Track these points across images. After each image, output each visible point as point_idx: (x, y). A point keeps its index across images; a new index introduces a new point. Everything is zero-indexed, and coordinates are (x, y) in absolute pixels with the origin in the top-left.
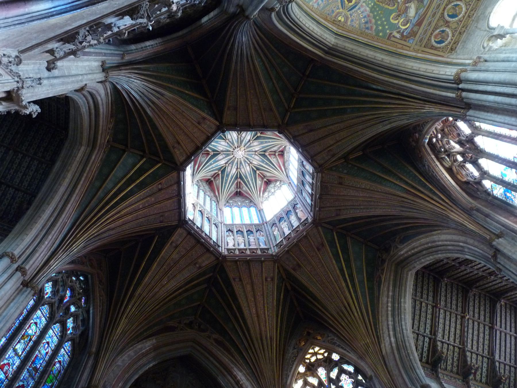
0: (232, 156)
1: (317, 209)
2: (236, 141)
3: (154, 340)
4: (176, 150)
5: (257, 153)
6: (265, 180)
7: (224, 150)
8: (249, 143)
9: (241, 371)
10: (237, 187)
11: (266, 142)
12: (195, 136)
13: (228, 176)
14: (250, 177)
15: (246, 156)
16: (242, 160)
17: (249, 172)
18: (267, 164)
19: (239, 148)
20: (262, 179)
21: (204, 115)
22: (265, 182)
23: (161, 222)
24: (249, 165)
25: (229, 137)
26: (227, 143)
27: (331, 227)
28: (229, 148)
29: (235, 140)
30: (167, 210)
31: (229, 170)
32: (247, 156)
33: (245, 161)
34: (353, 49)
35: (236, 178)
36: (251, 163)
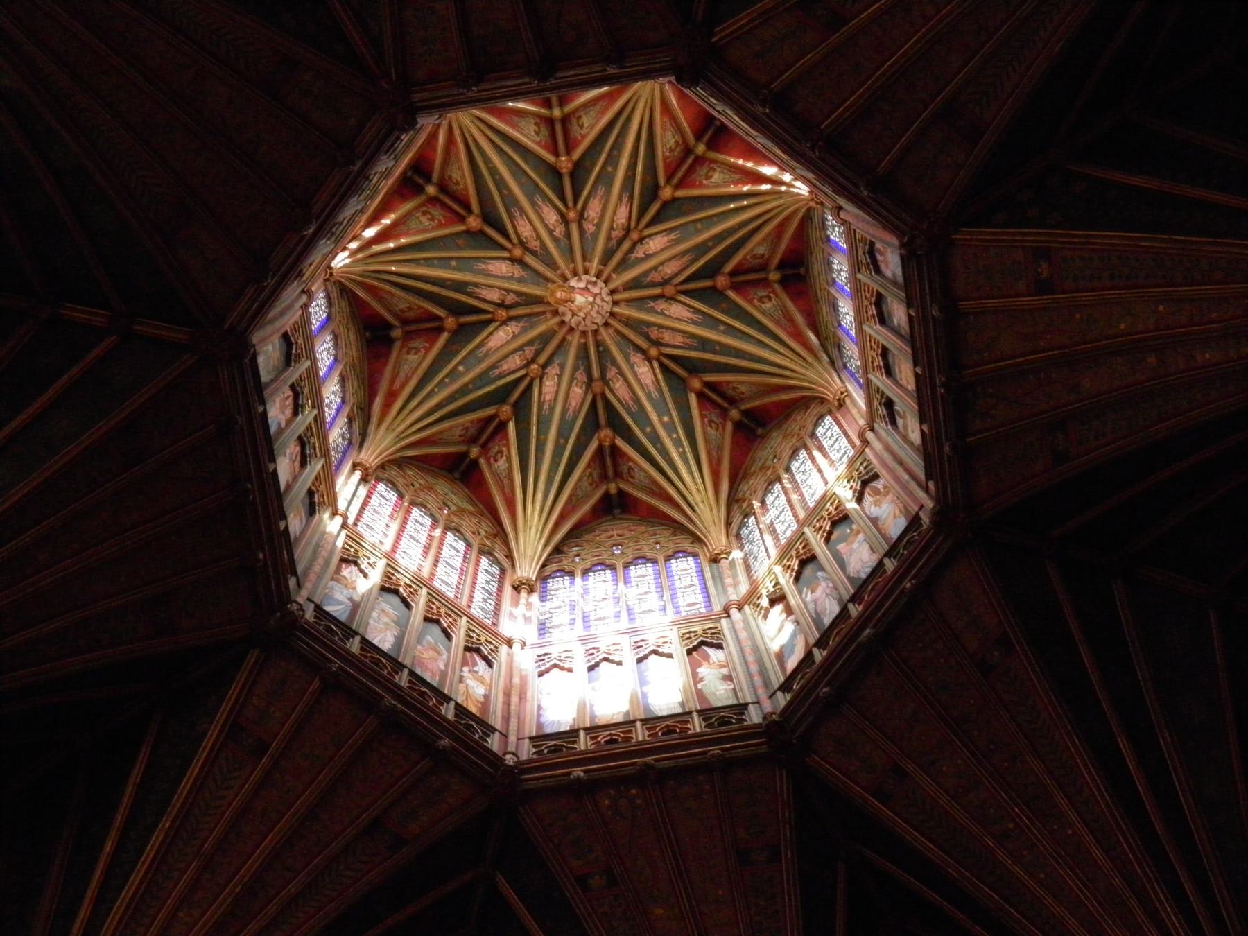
0: (605, 335)
1: (611, 70)
2: (532, 327)
5: (572, 215)
6: (701, 149)
7: (581, 376)
8: (529, 259)
10: (764, 283)
11: (500, 183)
13: (704, 344)
14: (698, 232)
15: (595, 265)
16: (618, 281)
17: (672, 236)
18: (613, 160)
19: (561, 309)
20: (700, 160)
22: (711, 146)
24: (641, 240)
25: (516, 361)
26: (544, 366)
28: (566, 354)
29: (524, 330)
31: (679, 339)
32: (596, 261)
33: (624, 265)
35: (712, 296)
36: (628, 230)
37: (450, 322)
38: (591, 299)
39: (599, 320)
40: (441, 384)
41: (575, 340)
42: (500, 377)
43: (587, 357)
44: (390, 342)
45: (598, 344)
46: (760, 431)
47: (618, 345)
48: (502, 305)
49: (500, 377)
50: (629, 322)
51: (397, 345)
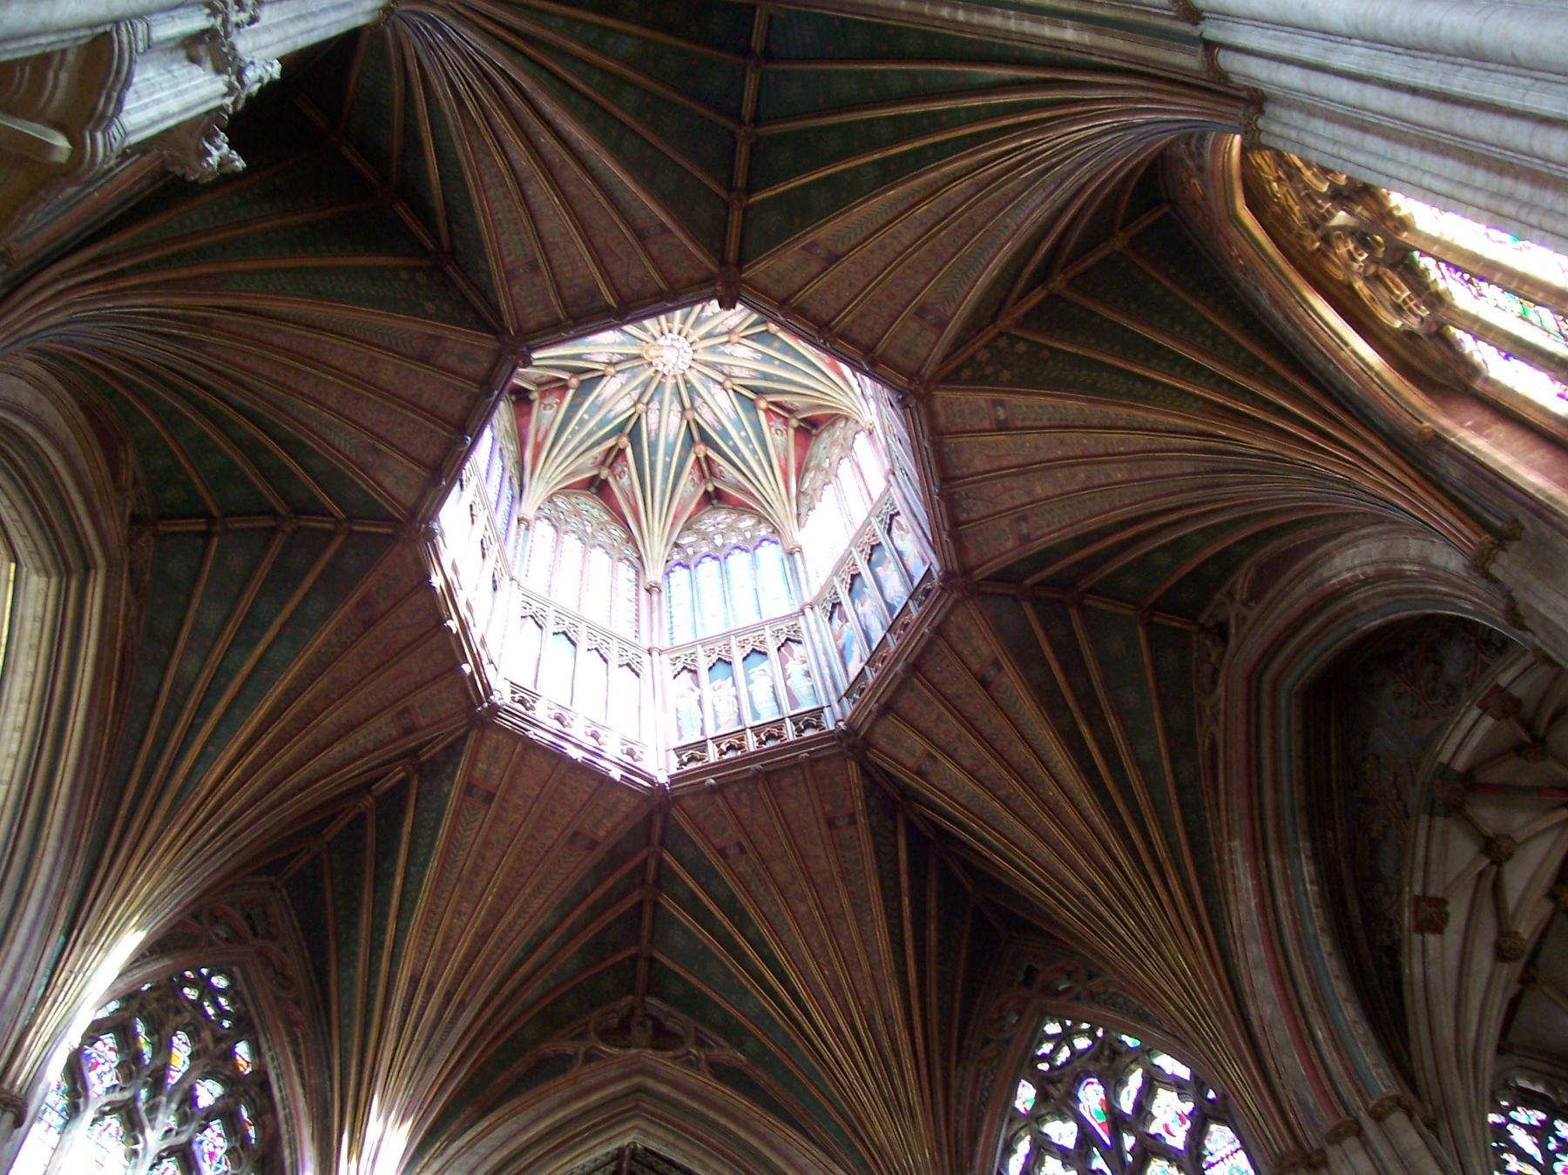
0: (693, 377)
2: (634, 377)
3: (1236, 843)
4: (602, 833)
7: (676, 407)
9: (1329, 556)
12: (538, 789)
13: (766, 376)
16: (695, 336)
21: (454, 790)
23: (853, 819)
25: (627, 403)
27: (736, 218)
28: (663, 393)
29: (629, 380)
30: (811, 810)
31: (745, 373)
34: (22, 536)
37: (574, 382)
38: (676, 352)
39: (685, 367)
40: (574, 433)
41: (670, 382)
42: (616, 417)
43: (679, 393)
44: (530, 403)
45: (686, 382)
46: (814, 431)
47: (700, 380)
48: (610, 364)
49: (616, 417)
50: (706, 364)
51: (536, 405)
